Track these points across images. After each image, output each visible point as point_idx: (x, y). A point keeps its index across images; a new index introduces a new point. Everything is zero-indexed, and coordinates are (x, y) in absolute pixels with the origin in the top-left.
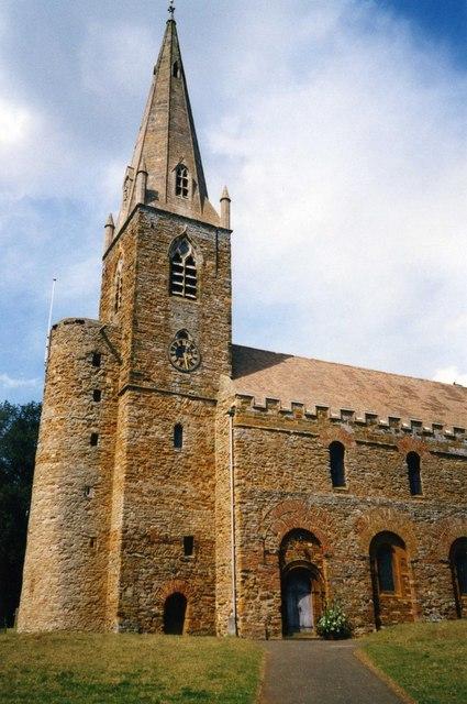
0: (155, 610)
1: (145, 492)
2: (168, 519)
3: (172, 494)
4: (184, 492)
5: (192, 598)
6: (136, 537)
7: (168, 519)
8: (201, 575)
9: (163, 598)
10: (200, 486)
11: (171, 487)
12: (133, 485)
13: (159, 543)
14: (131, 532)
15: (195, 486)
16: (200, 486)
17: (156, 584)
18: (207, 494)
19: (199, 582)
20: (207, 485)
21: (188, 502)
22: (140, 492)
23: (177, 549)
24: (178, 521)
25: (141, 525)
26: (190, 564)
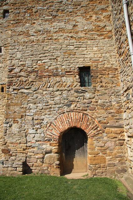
0: (47, 146)
1: (31, 33)
2: (58, 53)
3: (61, 30)
4: (75, 26)
5: (93, 132)
6: (22, 73)
7: (58, 53)
8: (102, 106)
9: (56, 134)
10: (94, 17)
11: (59, 24)
12: (20, 29)
13: (49, 76)
14: (17, 70)
15: (87, 20)
16: (94, 17)
17: (47, 119)
18: (102, 24)
19: (101, 114)
20: (102, 17)
21: (81, 35)
22: (28, 35)
23: (73, 80)
24: (71, 54)
25: (28, 62)
26: (87, 95)
